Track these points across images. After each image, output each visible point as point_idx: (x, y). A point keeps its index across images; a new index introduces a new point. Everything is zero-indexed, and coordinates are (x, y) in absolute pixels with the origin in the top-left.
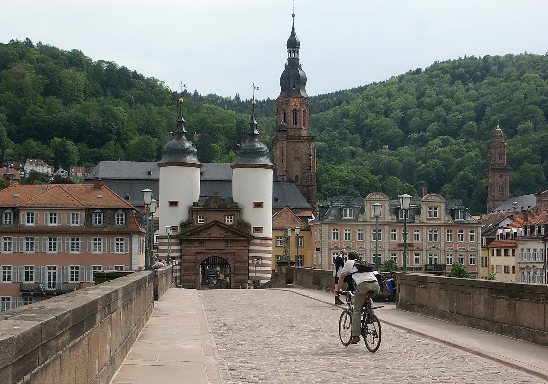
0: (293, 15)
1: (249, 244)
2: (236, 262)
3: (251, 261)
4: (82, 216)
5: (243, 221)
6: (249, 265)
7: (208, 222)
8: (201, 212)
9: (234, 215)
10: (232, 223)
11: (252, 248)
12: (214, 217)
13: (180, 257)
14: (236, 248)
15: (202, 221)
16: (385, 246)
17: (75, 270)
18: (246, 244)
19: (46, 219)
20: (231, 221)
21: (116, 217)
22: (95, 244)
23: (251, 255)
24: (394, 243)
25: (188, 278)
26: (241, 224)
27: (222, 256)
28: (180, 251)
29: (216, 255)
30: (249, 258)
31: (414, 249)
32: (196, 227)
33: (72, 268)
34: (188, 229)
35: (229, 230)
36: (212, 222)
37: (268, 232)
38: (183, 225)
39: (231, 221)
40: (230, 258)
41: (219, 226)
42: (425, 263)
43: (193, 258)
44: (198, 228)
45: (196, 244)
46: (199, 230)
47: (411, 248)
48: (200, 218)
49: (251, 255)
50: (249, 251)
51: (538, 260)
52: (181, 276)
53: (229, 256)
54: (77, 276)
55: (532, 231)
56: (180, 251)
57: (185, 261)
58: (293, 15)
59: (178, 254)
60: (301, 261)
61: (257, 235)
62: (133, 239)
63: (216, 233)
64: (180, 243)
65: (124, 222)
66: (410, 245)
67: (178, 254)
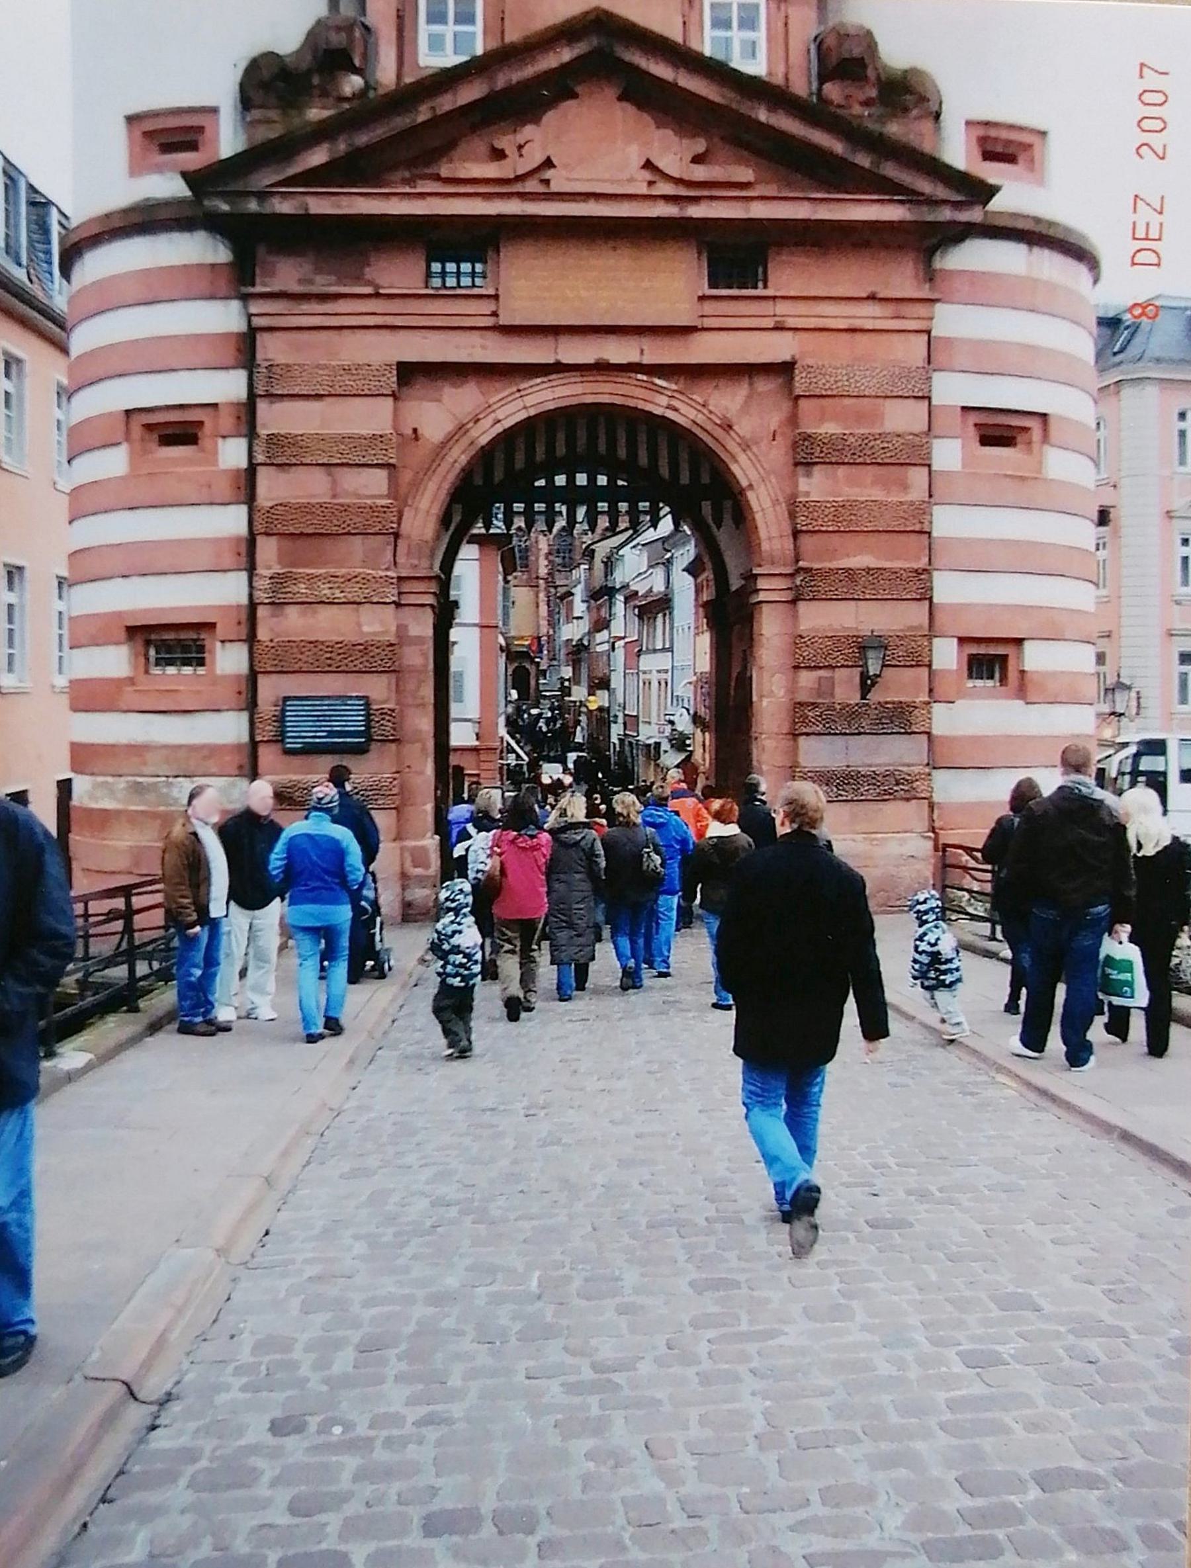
2: (806, 454)
3: (948, 454)
14: (809, 313)
18: (901, 278)
25: (330, 625)
27: (664, 400)
29: (603, 392)
36: (567, 32)
40: (744, 427)
43: (371, 417)
45: (400, 273)
52: (253, 606)
53: (727, 400)
57: (284, 453)
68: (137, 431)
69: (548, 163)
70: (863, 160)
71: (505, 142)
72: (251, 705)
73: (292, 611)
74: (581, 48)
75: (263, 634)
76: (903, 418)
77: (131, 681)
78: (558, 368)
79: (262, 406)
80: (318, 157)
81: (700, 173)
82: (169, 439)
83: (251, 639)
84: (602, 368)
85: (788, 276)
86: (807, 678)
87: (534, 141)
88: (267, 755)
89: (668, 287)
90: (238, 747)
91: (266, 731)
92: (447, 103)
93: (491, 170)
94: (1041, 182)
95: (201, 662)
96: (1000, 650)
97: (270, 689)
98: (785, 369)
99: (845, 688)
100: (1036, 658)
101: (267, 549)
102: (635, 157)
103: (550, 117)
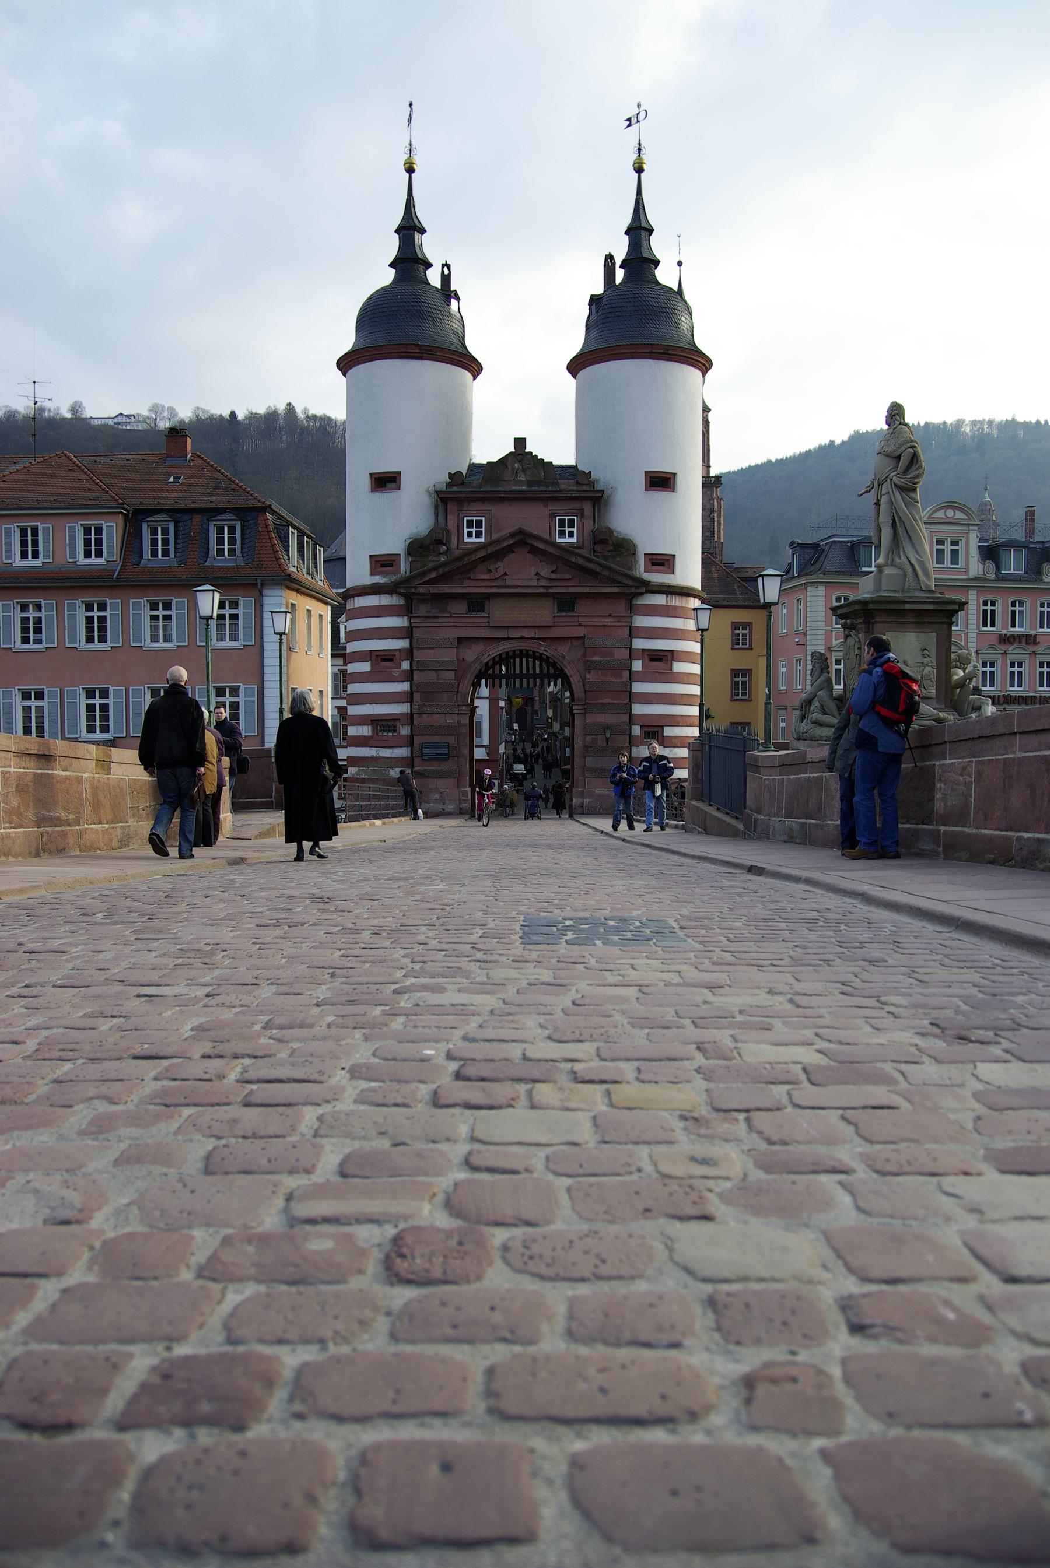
0: (680, 264)
1: (633, 610)
3: (637, 665)
4: (113, 530)
5: (610, 531)
6: (632, 677)
7: (495, 537)
8: (479, 506)
9: (581, 514)
10: (574, 540)
11: (642, 621)
12: (516, 518)
13: (409, 654)
15: (479, 535)
16: (967, 642)
17: (97, 701)
18: (620, 608)
19: (9, 544)
20: (571, 534)
21: (213, 536)
22: (155, 618)
23: (639, 644)
24: (990, 633)
25: (437, 720)
26: (603, 542)
27: (542, 649)
28: (408, 632)
29: (524, 646)
30: (632, 654)
31: (1039, 649)
32: (457, 553)
33: (90, 694)
34: (432, 561)
35: (567, 563)
37: (690, 572)
38: (417, 548)
39: (571, 534)
41: (534, 551)
43: (449, 655)
44: (461, 558)
45: (460, 608)
46: (468, 563)
47: (1031, 648)
48: (470, 524)
49: (639, 644)
50: (634, 632)
52: (412, 714)
53: (563, 649)
54: (105, 718)
56: (408, 632)
57: (423, 666)
58: (680, 264)
59: (401, 644)
60: (744, 683)
61: (657, 578)
62: (267, 600)
63: (523, 572)
64: (406, 610)
65: (238, 547)
66: (1030, 640)
67: (401, 644)
68: (374, 657)
69: (505, 574)
70: (606, 573)
71: (491, 568)
72: (412, 746)
73: (425, 716)
74: (516, 539)
75: (415, 723)
76: (621, 654)
77: (372, 737)
78: (509, 638)
79: (415, 651)
80: (433, 575)
81: (554, 576)
82: (384, 660)
83: (412, 724)
84: (522, 638)
85: (582, 608)
86: (589, 738)
87: (502, 566)
88: (416, 761)
89: (543, 613)
90: (407, 758)
91: (417, 753)
92: (473, 558)
93: (487, 577)
94: (673, 573)
95: (395, 731)
96: (656, 729)
97: (417, 740)
98: (583, 638)
99: (601, 742)
100: (668, 731)
101: (417, 696)
102: (533, 572)
103: (506, 559)
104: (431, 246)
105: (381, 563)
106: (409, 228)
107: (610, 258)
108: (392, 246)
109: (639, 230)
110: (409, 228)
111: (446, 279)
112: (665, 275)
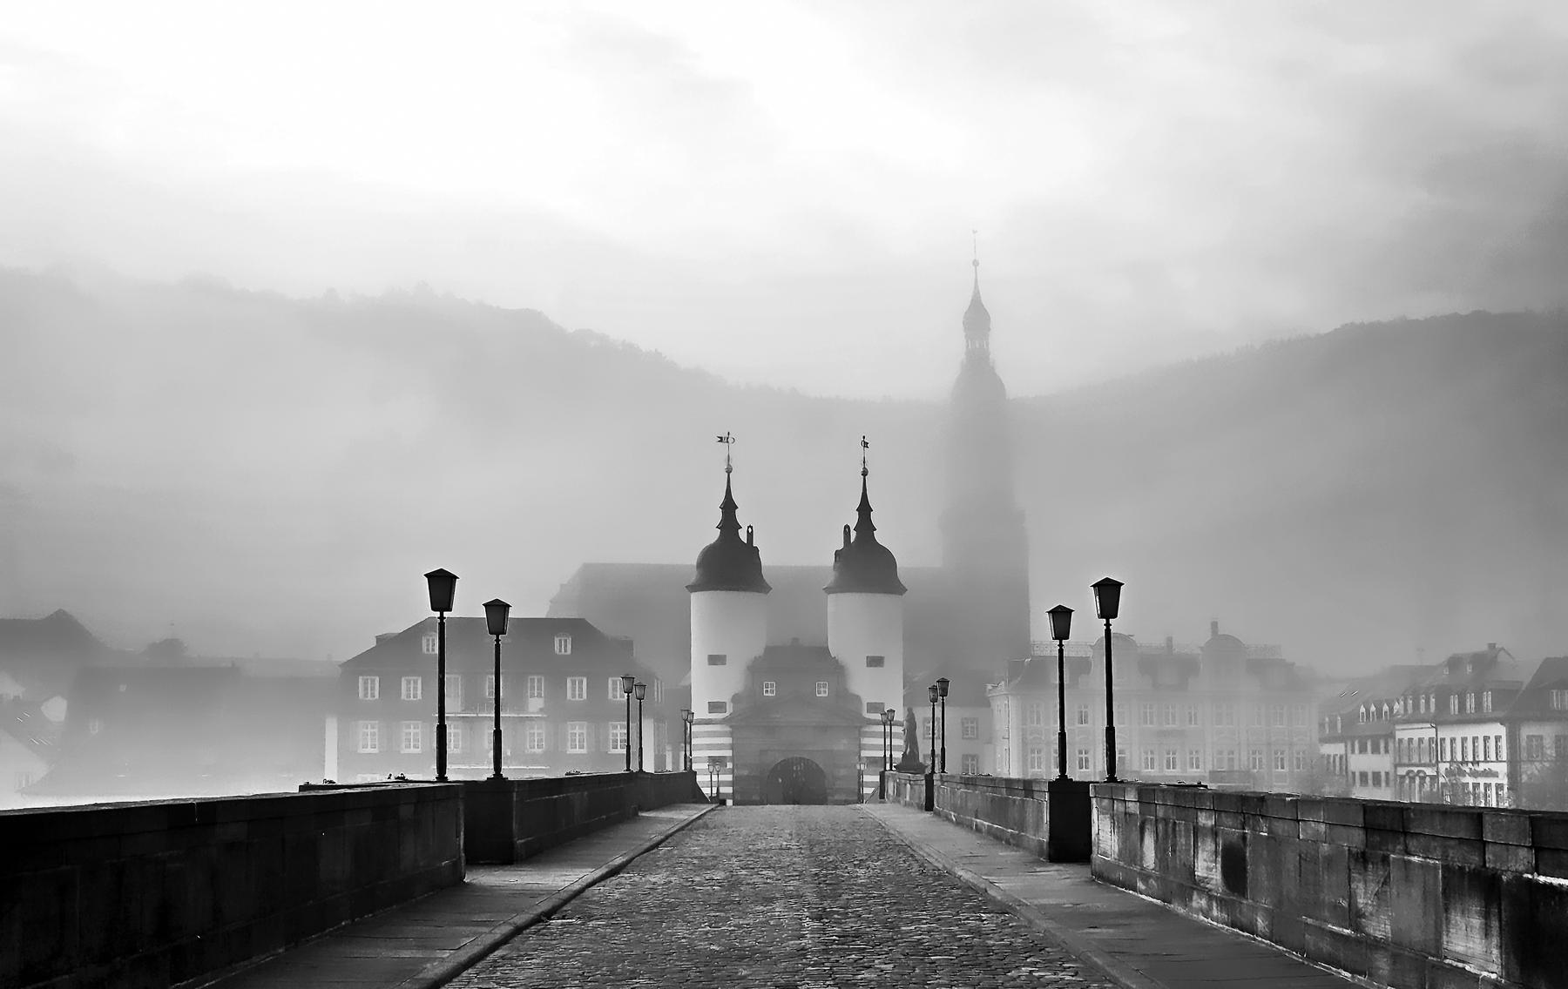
11: (865, 741)
23: (865, 754)
28: (732, 747)
38: (736, 699)
42: (1209, 767)
51: (1426, 760)
55: (1416, 706)
104: (741, 517)
105: (715, 707)
106: (729, 506)
107: (847, 527)
108: (718, 516)
109: (865, 509)
110: (729, 506)
111: (750, 535)
112: (879, 537)
